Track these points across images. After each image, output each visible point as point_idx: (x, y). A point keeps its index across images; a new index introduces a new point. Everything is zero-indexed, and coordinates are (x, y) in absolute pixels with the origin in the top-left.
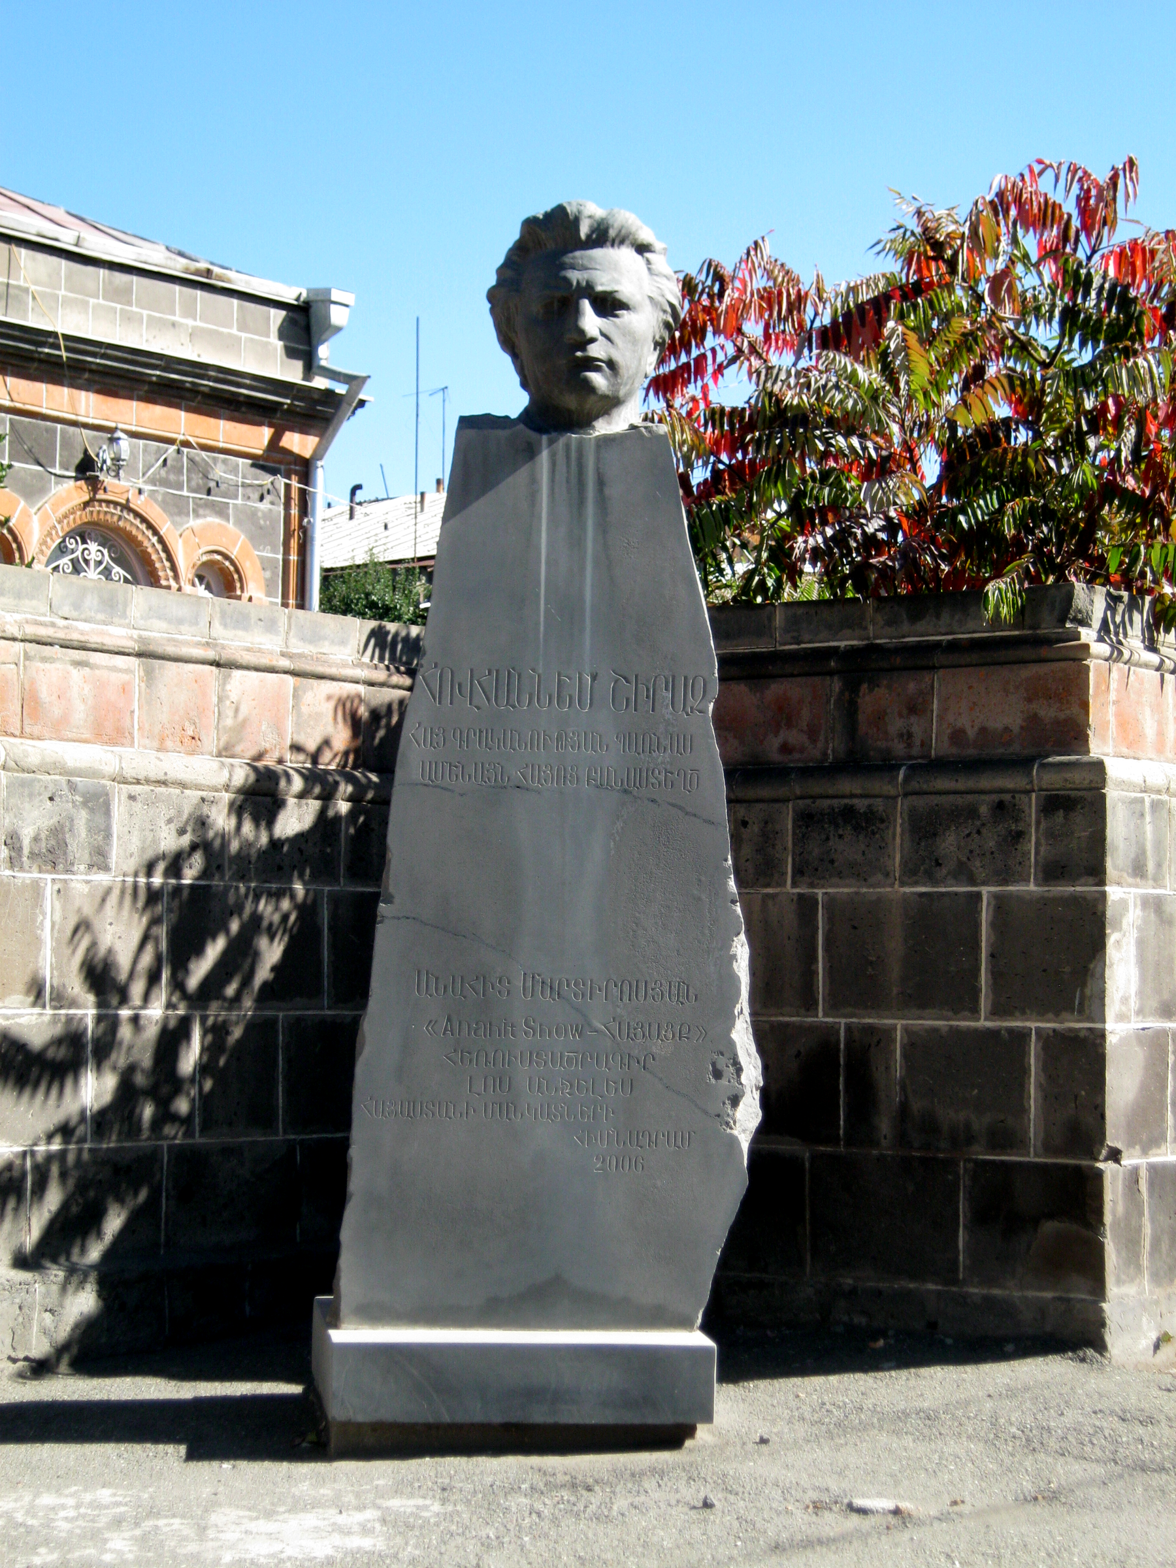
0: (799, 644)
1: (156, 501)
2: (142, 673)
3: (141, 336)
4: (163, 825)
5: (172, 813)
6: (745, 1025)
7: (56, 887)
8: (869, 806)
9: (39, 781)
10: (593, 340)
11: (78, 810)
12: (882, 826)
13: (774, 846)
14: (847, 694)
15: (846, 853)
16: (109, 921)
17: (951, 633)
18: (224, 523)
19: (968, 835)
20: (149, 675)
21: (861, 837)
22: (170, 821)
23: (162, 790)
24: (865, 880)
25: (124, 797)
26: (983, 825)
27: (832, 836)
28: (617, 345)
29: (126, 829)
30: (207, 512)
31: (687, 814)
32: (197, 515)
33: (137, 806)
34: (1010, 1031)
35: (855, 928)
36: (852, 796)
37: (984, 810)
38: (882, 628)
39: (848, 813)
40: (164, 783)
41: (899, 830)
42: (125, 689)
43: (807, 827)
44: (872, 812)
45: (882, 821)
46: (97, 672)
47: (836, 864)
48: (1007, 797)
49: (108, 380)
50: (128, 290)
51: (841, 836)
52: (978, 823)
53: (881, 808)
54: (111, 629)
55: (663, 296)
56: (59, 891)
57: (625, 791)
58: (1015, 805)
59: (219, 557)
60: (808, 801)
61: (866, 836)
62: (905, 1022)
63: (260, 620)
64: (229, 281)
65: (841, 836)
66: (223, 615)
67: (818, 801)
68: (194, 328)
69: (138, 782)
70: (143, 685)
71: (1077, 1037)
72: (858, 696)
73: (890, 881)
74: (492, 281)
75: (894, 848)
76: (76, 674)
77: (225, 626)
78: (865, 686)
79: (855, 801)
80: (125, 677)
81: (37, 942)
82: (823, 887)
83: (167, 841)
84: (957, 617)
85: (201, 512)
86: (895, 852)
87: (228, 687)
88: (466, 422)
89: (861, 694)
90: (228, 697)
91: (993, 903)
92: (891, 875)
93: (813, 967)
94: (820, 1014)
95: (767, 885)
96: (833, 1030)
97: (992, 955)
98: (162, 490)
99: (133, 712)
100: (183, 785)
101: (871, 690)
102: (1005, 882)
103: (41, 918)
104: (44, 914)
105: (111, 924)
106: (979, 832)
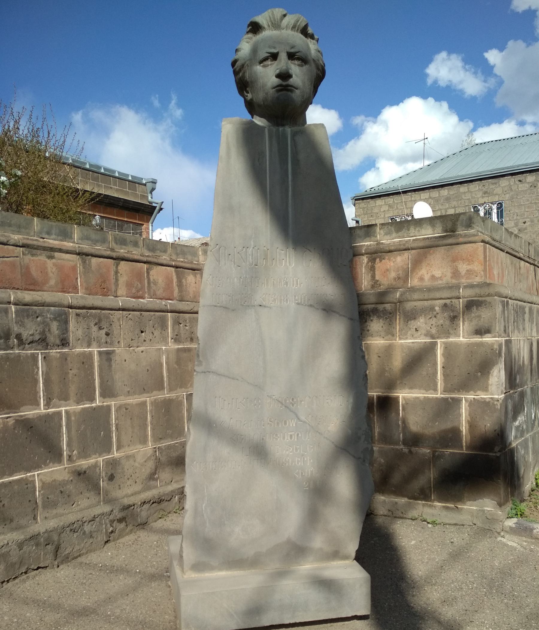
2: (81, 262)
4: (93, 326)
5: (97, 321)
7: (43, 356)
9: (32, 309)
11: (52, 321)
16: (70, 368)
17: (415, 236)
19: (430, 318)
20: (84, 262)
21: (381, 320)
22: (96, 324)
25: (74, 315)
26: (438, 314)
29: (76, 329)
33: (80, 319)
34: (453, 399)
35: (379, 357)
37: (437, 308)
42: (74, 268)
44: (385, 310)
46: (59, 261)
48: (448, 301)
52: (435, 313)
54: (65, 243)
56: (45, 358)
58: (452, 305)
69: (79, 308)
70: (81, 267)
71: (485, 401)
72: (374, 263)
73: (394, 338)
76: (50, 263)
77: (117, 244)
78: (378, 260)
80: (72, 263)
81: (36, 381)
83: (95, 333)
84: (417, 229)
86: (396, 326)
87: (119, 268)
90: (119, 273)
91: (443, 346)
92: (395, 335)
97: (443, 367)
99: (77, 279)
101: (381, 261)
102: (448, 337)
103: (37, 370)
104: (38, 368)
105: (71, 370)
106: (435, 317)
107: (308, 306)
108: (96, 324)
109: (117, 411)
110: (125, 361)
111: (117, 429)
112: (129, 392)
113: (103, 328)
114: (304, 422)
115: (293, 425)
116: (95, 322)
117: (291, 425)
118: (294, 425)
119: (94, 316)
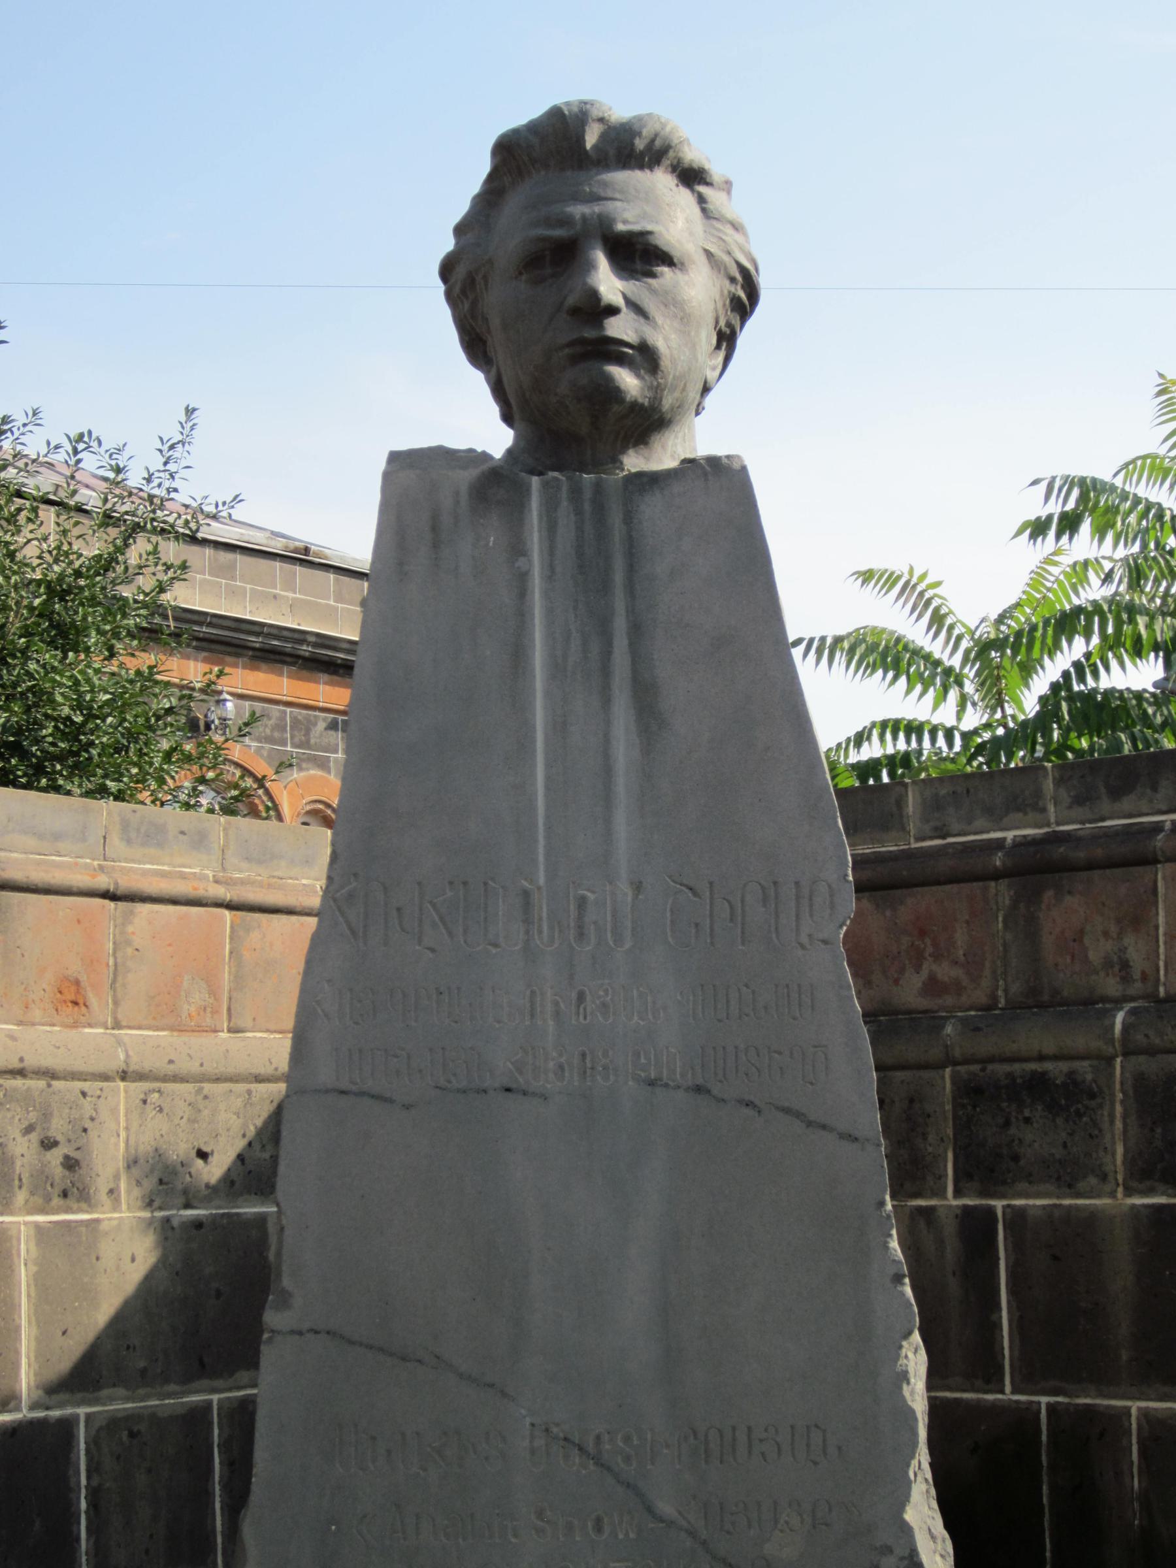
0: (944, 838)
1: (262, 756)
3: (245, 607)
4: (17, 1134)
5: (33, 1117)
6: (924, 1487)
8: (1071, 1074)
10: (613, 311)
12: (1093, 1103)
13: (924, 1136)
14: (1022, 905)
15: (1036, 1145)
18: (325, 775)
21: (1060, 1121)
22: (29, 1129)
23: (18, 1082)
24: (1070, 1186)
27: (1013, 1120)
28: (655, 323)
30: (310, 765)
31: (809, 1124)
32: (301, 769)
36: (1041, 1058)
38: (1070, 807)
39: (1038, 1085)
40: (21, 1073)
41: (1119, 1109)
43: (974, 1107)
45: (1092, 1096)
47: (1022, 1163)
49: (213, 646)
50: (232, 566)
51: (1027, 1120)
53: (1089, 1077)
55: (729, 253)
57: (699, 1089)
59: (321, 806)
60: (975, 1068)
61: (1067, 1121)
62: (1143, 1404)
63: (183, 833)
64: (326, 558)
65: (1027, 1120)
66: (125, 826)
67: (990, 1067)
68: (293, 599)
73: (1108, 1188)
74: (448, 244)
75: (1113, 1137)
77: (129, 841)
79: (1048, 1066)
82: (1002, 1196)
83: (25, 1160)
85: (304, 765)
88: (395, 458)
89: (1043, 906)
92: (1111, 1177)
93: (994, 1317)
94: (1008, 1388)
95: (917, 1195)
96: (1025, 1417)
98: (267, 746)
100: (50, 1075)
107: (687, 1089)
108: (29, 1129)
109: (94, 1443)
110: (133, 1260)
111: (94, 1505)
112: (143, 1372)
113: (55, 1144)
114: (671, 1524)
115: (627, 1534)
116: (25, 1124)
117: (621, 1536)
118: (632, 1535)
119: (27, 1099)
